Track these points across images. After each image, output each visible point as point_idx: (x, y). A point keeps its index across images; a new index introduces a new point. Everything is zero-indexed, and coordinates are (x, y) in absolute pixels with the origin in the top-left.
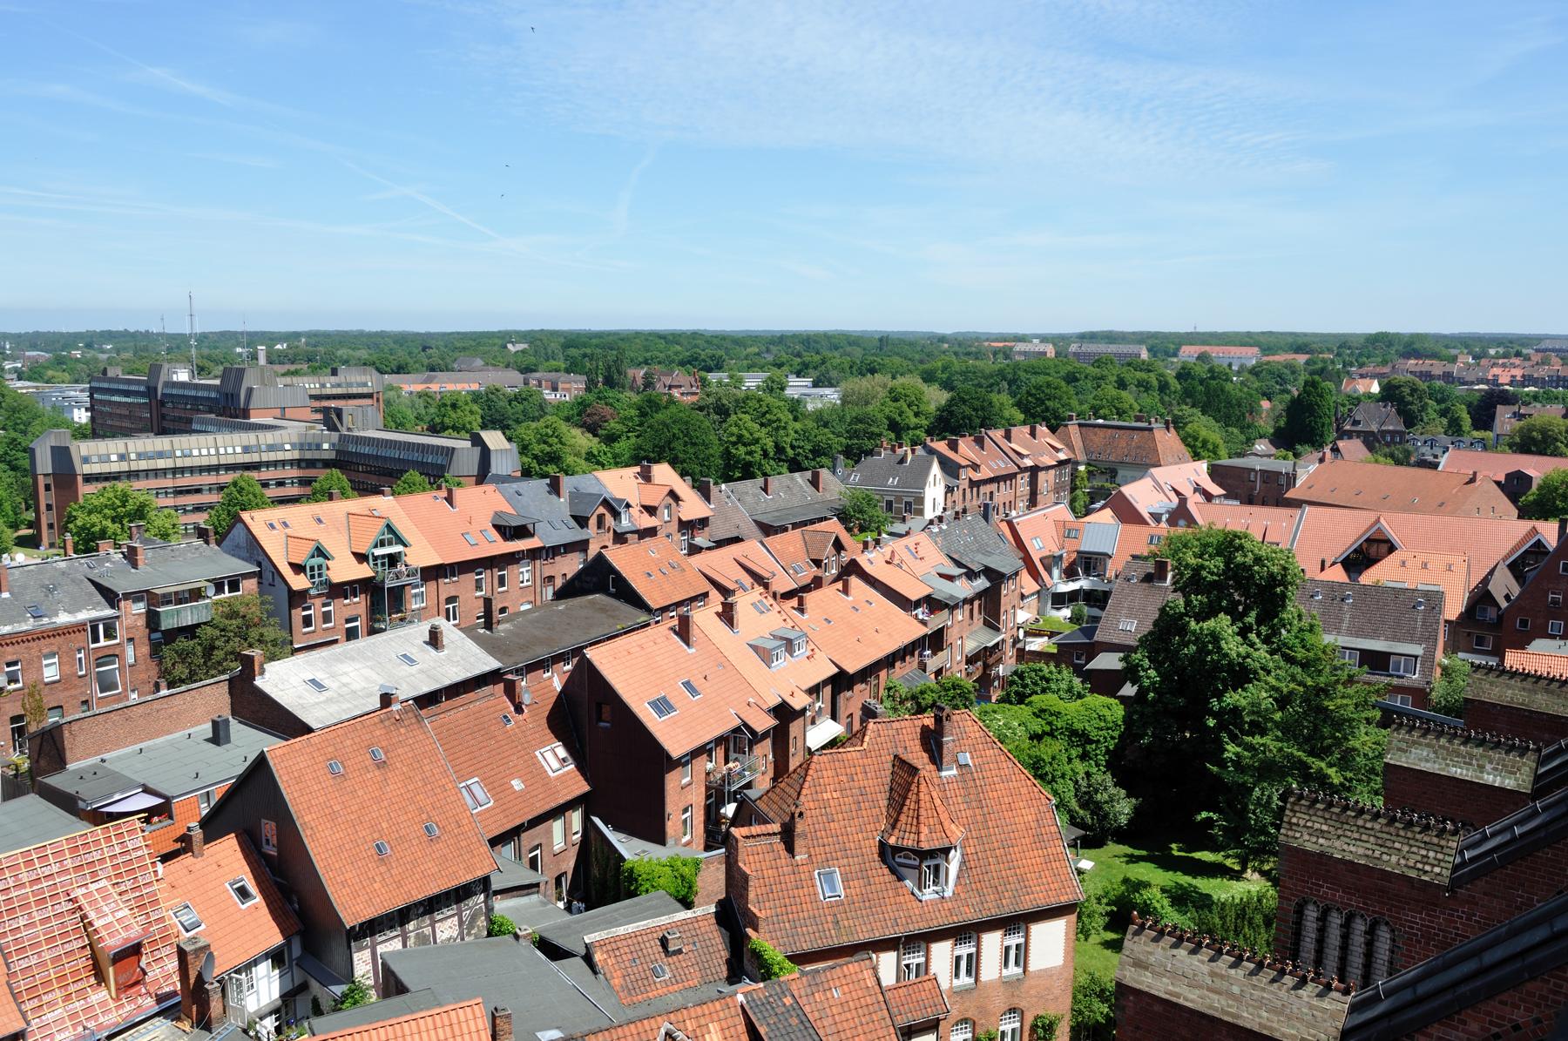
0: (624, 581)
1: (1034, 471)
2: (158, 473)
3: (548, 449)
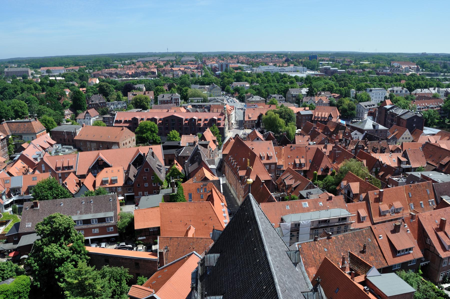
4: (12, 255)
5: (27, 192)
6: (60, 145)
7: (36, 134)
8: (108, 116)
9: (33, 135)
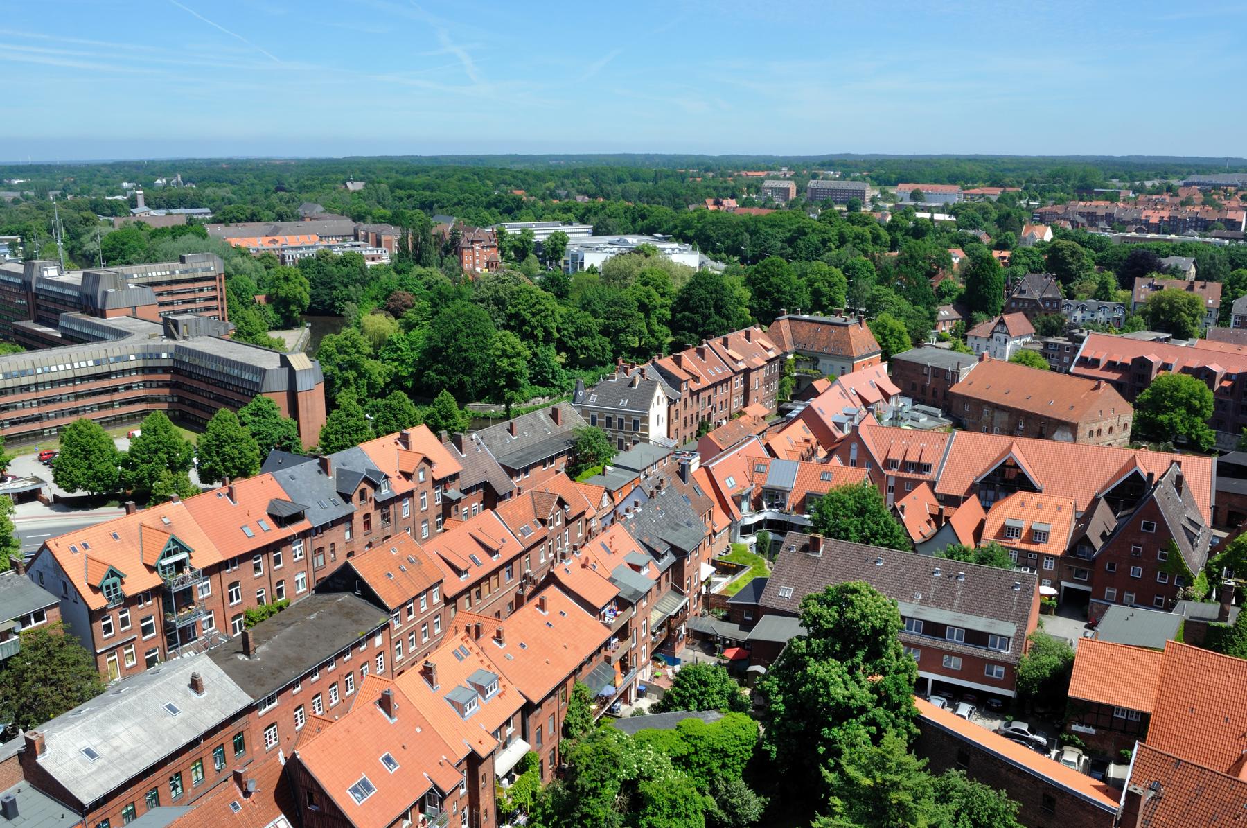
0: (367, 585)
1: (747, 372)
2: (25, 388)
3: (347, 358)
4: (731, 653)
5: (801, 508)
6: (908, 401)
7: (853, 359)
8: (1061, 340)
9: (846, 361)
